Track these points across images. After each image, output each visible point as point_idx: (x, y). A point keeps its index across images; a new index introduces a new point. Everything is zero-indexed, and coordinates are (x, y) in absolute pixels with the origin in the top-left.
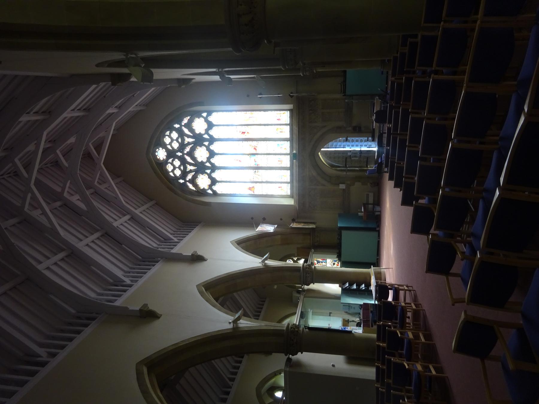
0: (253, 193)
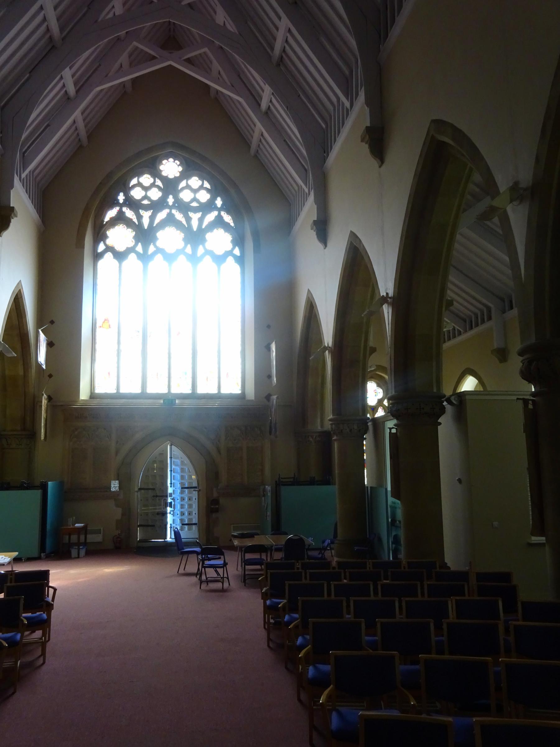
0: (98, 325)
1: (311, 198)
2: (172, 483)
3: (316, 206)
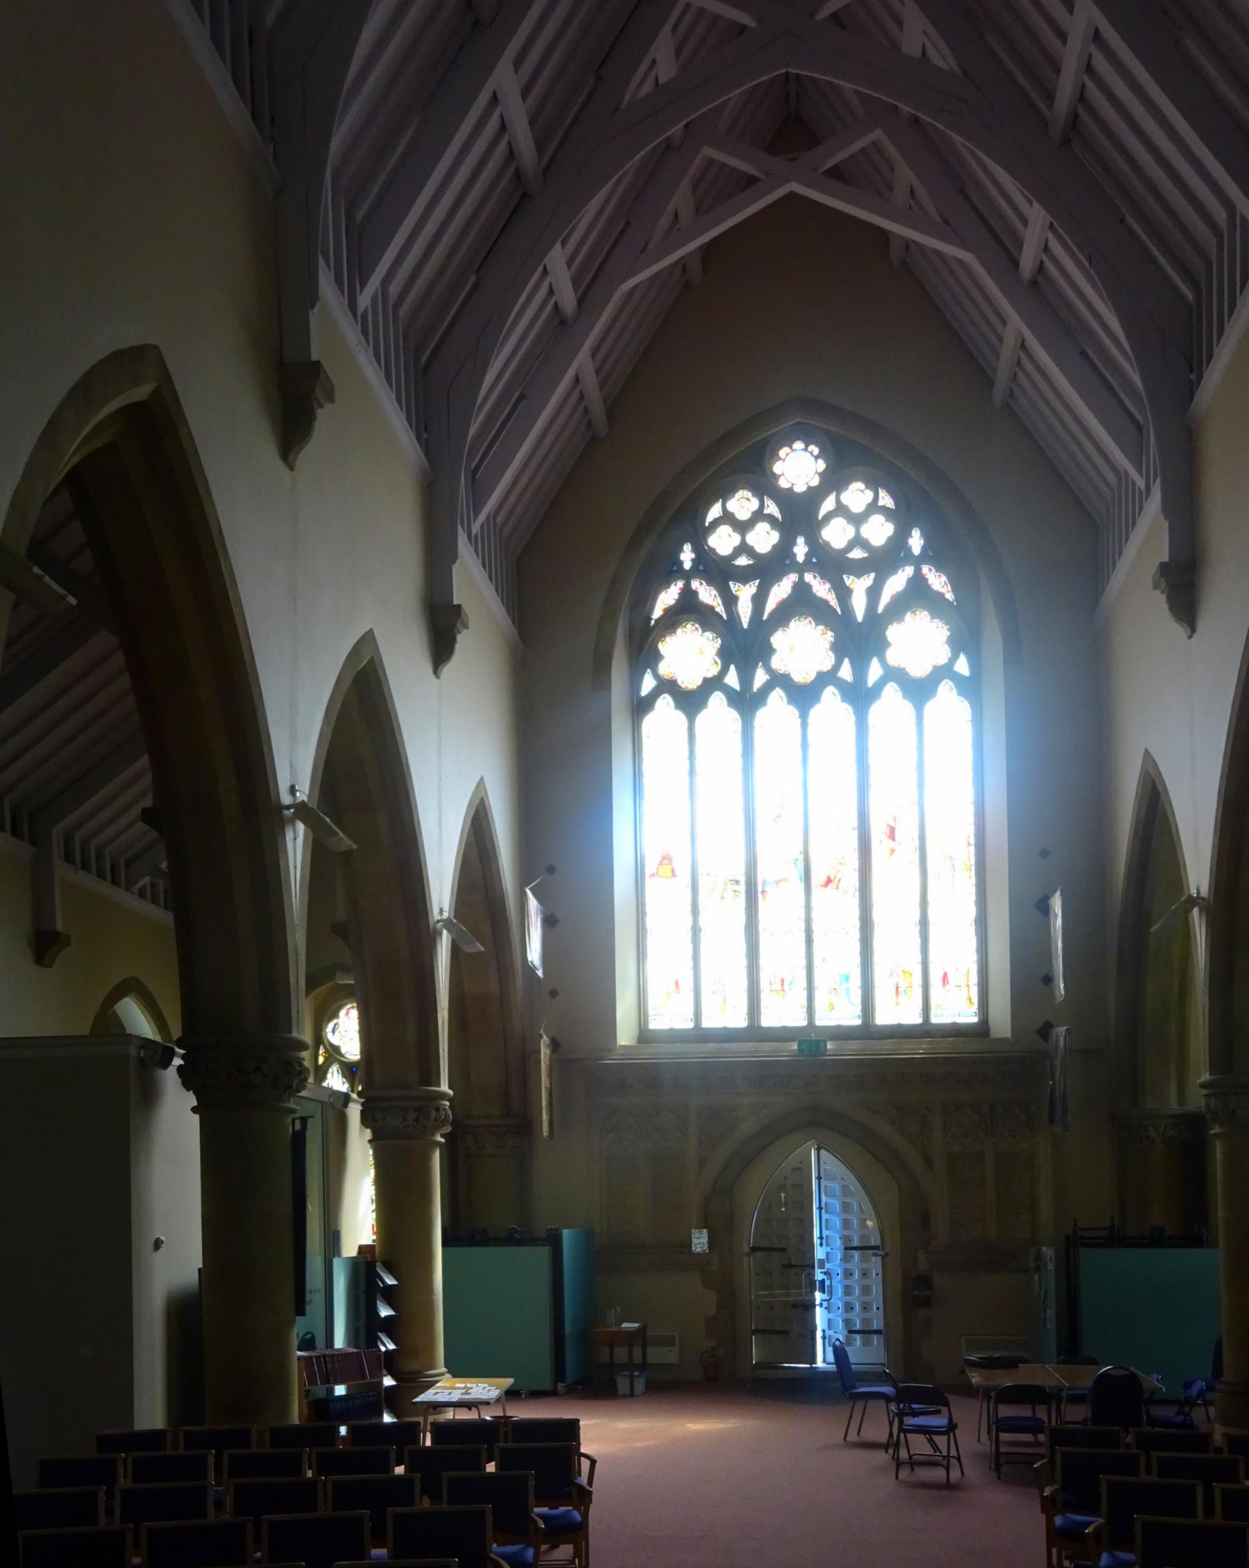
0: (648, 871)
1: (1155, 503)
2: (824, 1235)
3: (1166, 524)
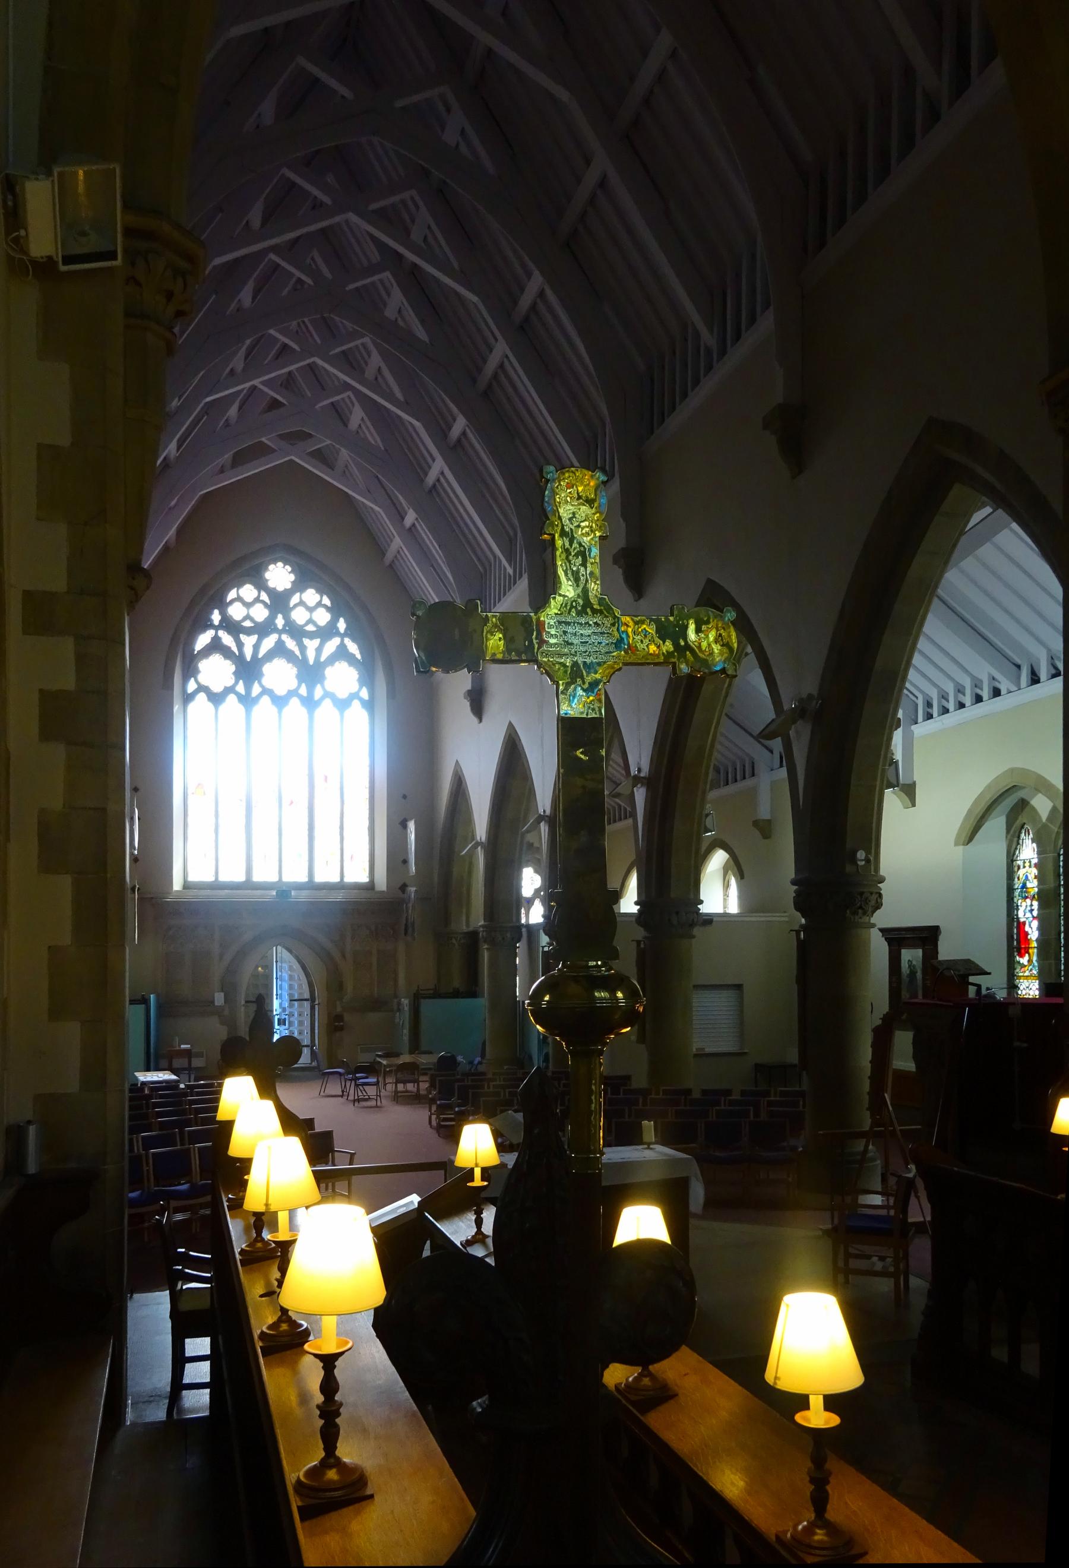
2: (279, 993)
